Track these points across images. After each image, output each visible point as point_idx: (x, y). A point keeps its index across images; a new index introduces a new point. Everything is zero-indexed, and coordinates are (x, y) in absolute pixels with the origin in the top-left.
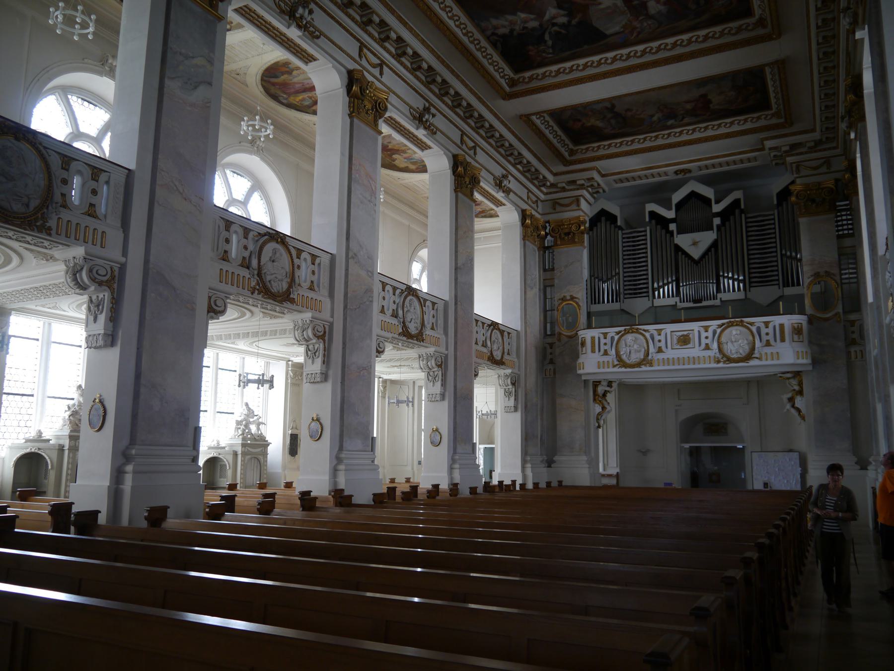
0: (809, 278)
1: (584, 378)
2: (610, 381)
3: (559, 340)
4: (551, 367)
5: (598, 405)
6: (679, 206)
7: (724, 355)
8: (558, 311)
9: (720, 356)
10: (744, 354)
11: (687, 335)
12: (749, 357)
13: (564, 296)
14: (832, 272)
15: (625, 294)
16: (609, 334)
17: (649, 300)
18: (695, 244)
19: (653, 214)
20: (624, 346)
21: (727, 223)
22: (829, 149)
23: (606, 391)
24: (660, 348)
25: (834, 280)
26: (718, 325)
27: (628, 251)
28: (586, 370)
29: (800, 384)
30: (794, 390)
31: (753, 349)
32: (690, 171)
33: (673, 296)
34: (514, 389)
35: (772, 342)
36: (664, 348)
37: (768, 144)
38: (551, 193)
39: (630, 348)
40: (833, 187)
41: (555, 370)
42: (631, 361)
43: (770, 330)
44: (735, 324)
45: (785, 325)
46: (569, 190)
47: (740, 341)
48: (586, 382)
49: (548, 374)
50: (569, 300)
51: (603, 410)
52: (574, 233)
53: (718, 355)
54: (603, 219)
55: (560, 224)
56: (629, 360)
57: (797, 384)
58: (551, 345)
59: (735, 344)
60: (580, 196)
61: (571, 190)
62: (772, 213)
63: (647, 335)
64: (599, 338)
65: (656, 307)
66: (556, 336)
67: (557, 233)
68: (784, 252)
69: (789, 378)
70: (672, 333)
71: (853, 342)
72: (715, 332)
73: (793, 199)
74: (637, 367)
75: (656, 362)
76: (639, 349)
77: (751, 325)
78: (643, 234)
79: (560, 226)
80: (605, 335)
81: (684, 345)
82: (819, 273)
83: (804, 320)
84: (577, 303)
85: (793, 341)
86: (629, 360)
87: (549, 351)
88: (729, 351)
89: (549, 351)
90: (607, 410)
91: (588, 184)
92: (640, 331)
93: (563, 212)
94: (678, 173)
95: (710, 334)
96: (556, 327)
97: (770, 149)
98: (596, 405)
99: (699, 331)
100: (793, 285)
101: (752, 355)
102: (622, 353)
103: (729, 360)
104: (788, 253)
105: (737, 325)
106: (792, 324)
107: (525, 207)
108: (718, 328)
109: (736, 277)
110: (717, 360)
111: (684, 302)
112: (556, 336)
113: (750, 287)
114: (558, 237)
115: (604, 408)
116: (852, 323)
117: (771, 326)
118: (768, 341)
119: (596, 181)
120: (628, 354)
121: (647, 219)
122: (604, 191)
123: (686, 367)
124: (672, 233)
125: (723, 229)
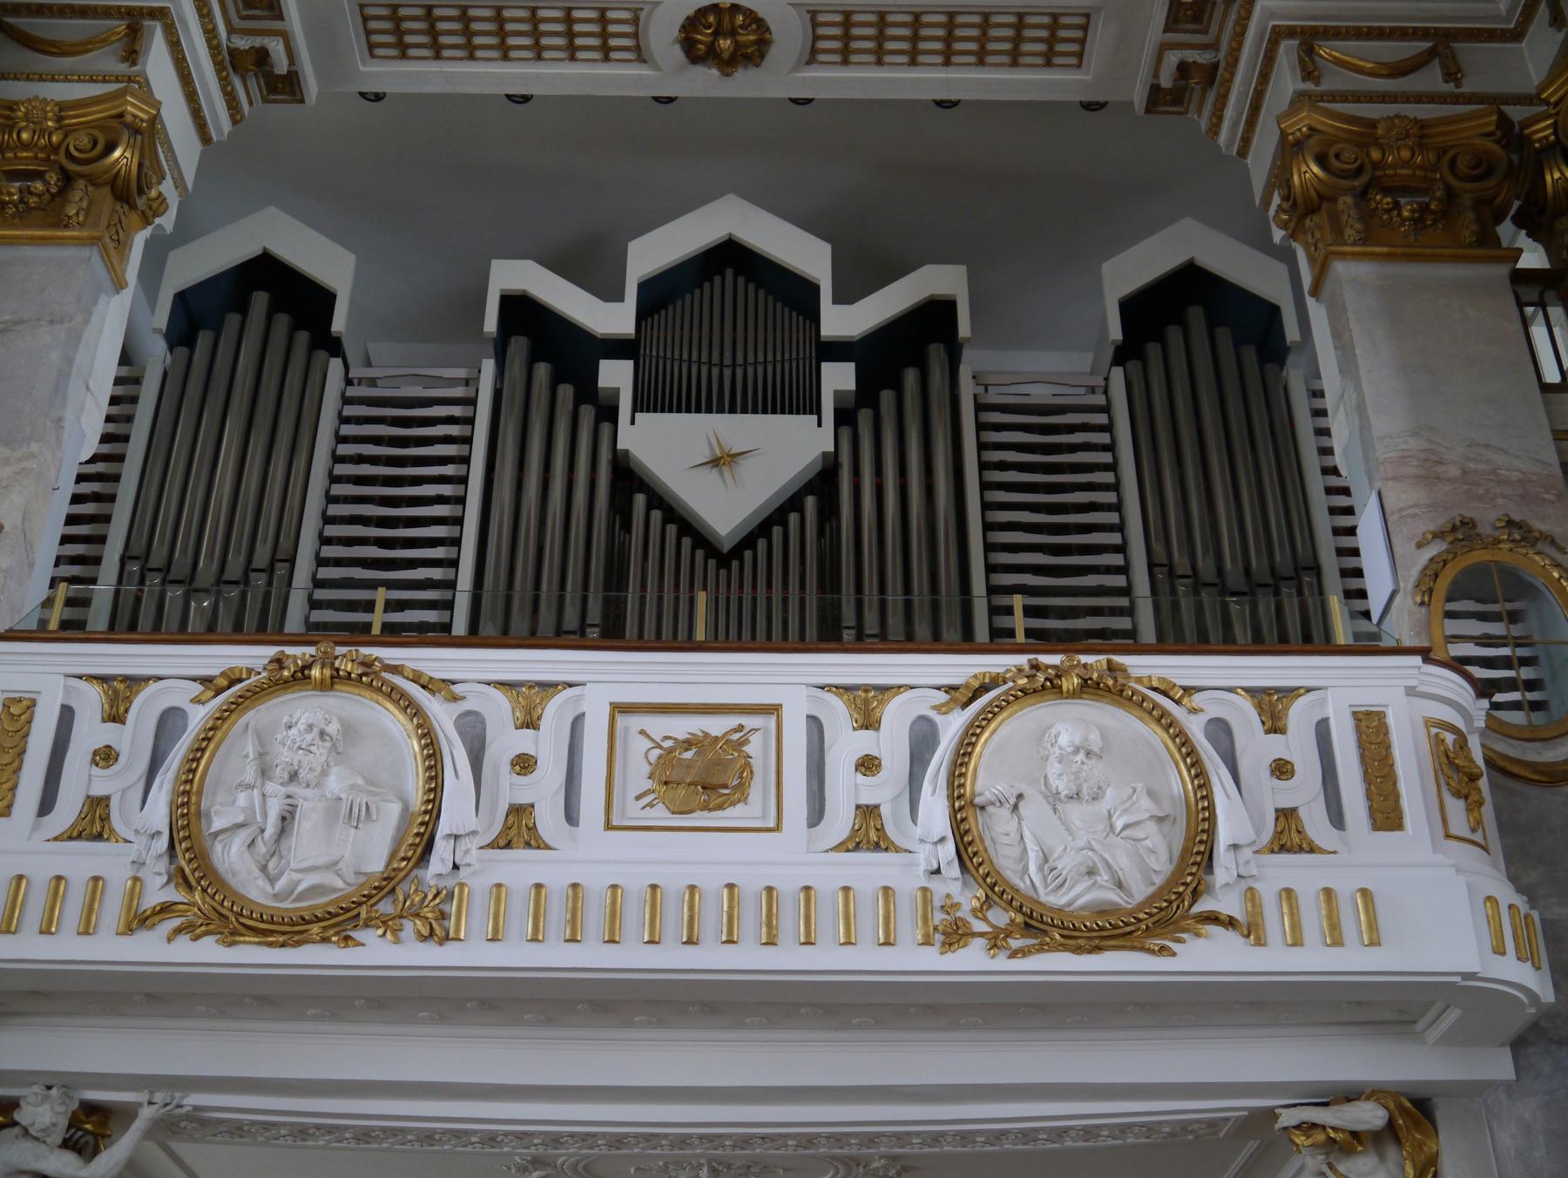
0: (1419, 546)
2: (91, 1109)
7: (996, 890)
9: (968, 898)
10: (1140, 891)
14: (1538, 525)
16: (153, 687)
18: (721, 461)
19: (519, 309)
20: (250, 774)
21: (887, 397)
24: (520, 812)
26: (951, 689)
27: (360, 459)
35: (1315, 822)
36: (548, 819)
39: (292, 789)
40: (1489, 144)
42: (281, 884)
43: (1298, 744)
45: (1391, 720)
47: (1109, 792)
53: (954, 888)
54: (260, 300)
56: (272, 880)
59: (1076, 813)
63: (442, 714)
64: (67, 715)
70: (621, 721)
72: (923, 740)
74: (325, 940)
76: (362, 799)
81: (706, 807)
82: (1468, 524)
85: (1448, 836)
86: (272, 880)
95: (891, 741)
99: (814, 723)
101: (1196, 895)
102: (218, 824)
110: (938, 917)
117: (1299, 715)
118: (1286, 815)
120: (271, 830)
121: (491, 324)
125: (864, 417)
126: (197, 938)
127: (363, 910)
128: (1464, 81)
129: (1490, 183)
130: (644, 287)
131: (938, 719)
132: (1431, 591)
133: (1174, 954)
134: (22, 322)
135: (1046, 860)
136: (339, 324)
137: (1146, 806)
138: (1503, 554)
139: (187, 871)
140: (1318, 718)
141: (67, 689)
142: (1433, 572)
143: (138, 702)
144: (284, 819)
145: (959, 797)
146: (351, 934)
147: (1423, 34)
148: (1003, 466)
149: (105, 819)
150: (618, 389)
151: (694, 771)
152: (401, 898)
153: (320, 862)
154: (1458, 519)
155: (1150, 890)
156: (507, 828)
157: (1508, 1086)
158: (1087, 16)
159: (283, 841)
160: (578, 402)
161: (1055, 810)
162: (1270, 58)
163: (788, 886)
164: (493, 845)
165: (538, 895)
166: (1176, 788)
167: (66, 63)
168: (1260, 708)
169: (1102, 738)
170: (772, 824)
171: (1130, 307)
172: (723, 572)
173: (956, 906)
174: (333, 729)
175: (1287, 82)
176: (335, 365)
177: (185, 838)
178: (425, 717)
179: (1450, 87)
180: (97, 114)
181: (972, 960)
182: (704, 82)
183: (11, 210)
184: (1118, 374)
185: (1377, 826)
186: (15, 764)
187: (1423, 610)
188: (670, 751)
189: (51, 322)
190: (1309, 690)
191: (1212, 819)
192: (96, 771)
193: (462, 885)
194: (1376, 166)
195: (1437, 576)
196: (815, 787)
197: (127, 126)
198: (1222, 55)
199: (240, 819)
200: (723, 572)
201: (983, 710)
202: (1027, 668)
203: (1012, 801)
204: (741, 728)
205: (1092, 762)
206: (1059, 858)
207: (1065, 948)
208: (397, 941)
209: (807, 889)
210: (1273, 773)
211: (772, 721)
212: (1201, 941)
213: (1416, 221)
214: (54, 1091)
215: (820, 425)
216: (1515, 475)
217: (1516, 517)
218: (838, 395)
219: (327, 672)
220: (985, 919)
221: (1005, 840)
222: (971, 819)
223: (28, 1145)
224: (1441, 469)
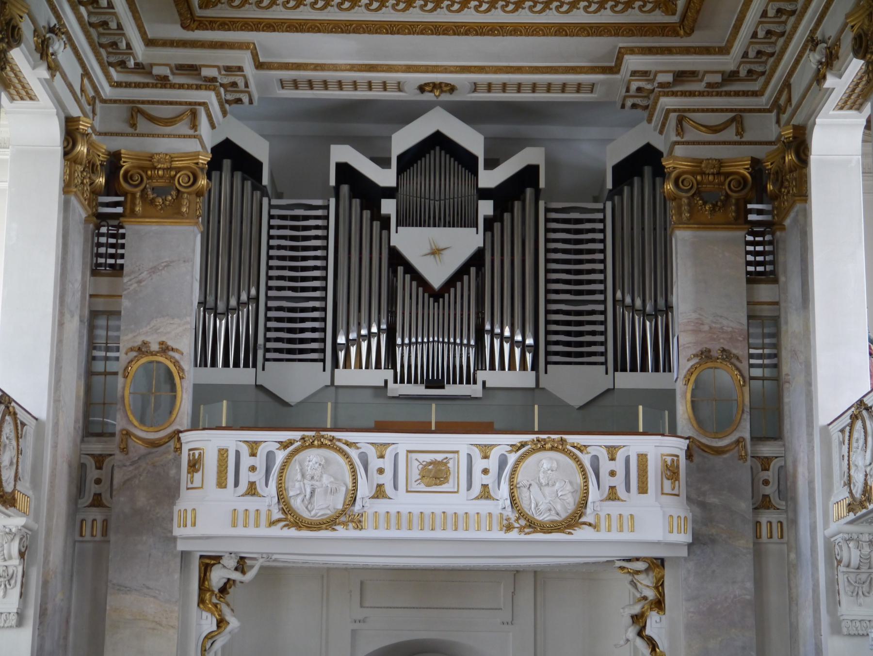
0: (688, 360)
1: (181, 546)
3: (124, 450)
4: (96, 514)
5: (209, 615)
6: (407, 161)
7: (522, 514)
8: (126, 377)
9: (512, 515)
10: (564, 515)
11: (443, 463)
12: (573, 521)
13: (145, 343)
14: (734, 351)
15: (267, 350)
16: (263, 445)
17: (324, 370)
18: (436, 252)
19: (345, 172)
20: (299, 477)
21: (507, 216)
22: (745, 94)
23: (229, 580)
25: (738, 369)
26: (512, 446)
27: (280, 247)
28: (201, 530)
29: (659, 586)
30: (645, 598)
31: (583, 503)
32: (452, 89)
33: (378, 366)
34: (20, 569)
35: (621, 491)
36: (389, 489)
37: (633, 62)
38: (128, 85)
39: (314, 482)
41: (105, 522)
42: (313, 513)
43: (619, 465)
44: (548, 446)
45: (649, 457)
46: (173, 86)
47: (557, 484)
48: (185, 556)
49: (87, 531)
50: (152, 354)
51: (218, 626)
52: (178, 191)
54: (227, 163)
55: (148, 164)
56: (310, 511)
57: (650, 585)
58: (100, 460)
59: (547, 490)
60: (200, 104)
61: (181, 86)
62: (600, 206)
63: (354, 454)
64: (238, 454)
65: (338, 387)
66: (118, 438)
67: (136, 186)
68: (619, 295)
69: (638, 572)
70: (410, 455)
71: (764, 504)
73: (669, 186)
74: (326, 529)
75: (371, 518)
76: (334, 486)
77: (581, 451)
78: (319, 213)
79: (144, 169)
81: (436, 484)
83: (681, 449)
84: (176, 363)
85: (663, 494)
86: (310, 511)
87: (93, 473)
88: (533, 506)
89: (93, 473)
90: (229, 628)
91: (225, 81)
92: (338, 443)
93: (153, 136)
94: (427, 88)
95: (492, 463)
96: (118, 416)
97: (634, 73)
98: (205, 614)
99: (469, 457)
100: (634, 369)
101: (580, 517)
102: (291, 493)
103: (533, 525)
104: (628, 300)
105: (553, 448)
106: (662, 455)
107: (75, 112)
108: (510, 452)
109: (519, 338)
110: (505, 522)
111: (402, 382)
112: (118, 438)
113: (547, 363)
114: (138, 195)
115: (221, 623)
116: (765, 463)
117: (620, 455)
118: (612, 488)
119: (244, 76)
120: (308, 497)
121: (332, 182)
122: (251, 102)
123: (439, 534)
124: (385, 222)
125: (497, 226)
126: (289, 528)
127: (337, 520)
128: (745, 135)
129: (746, 191)
130: (400, 158)
132: (689, 380)
134: (173, 262)
135: (537, 506)
136: (265, 181)
137: (569, 487)
139: (284, 508)
141: (237, 445)
143: (260, 448)
144: (312, 493)
145: (512, 485)
147: (732, 110)
148: (556, 251)
149: (255, 489)
151: (432, 473)
152: (348, 516)
153: (324, 506)
154: (704, 349)
155: (567, 514)
156: (377, 491)
157: (685, 558)
160: (372, 219)
161: (541, 489)
163: (461, 513)
164: (373, 497)
165: (388, 516)
167: (168, 130)
169: (557, 464)
170: (456, 490)
171: (616, 169)
174: (322, 463)
177: (283, 498)
178: (351, 459)
179: (737, 138)
185: (640, 493)
186: (225, 471)
187: (686, 387)
188: (425, 466)
189: (184, 261)
192: (250, 473)
195: (692, 374)
196: (469, 477)
198: (650, 102)
199: (298, 492)
200: (436, 304)
201: (523, 454)
202: (535, 439)
204: (447, 458)
206: (541, 505)
207: (541, 532)
209: (466, 513)
210: (609, 475)
211: (456, 455)
212: (581, 530)
213: (711, 211)
214: (233, 555)
215: (477, 233)
216: (730, 329)
217: (726, 348)
219: (319, 443)
220: (518, 523)
221: (525, 499)
222: (515, 492)
223: (225, 570)
224: (702, 327)
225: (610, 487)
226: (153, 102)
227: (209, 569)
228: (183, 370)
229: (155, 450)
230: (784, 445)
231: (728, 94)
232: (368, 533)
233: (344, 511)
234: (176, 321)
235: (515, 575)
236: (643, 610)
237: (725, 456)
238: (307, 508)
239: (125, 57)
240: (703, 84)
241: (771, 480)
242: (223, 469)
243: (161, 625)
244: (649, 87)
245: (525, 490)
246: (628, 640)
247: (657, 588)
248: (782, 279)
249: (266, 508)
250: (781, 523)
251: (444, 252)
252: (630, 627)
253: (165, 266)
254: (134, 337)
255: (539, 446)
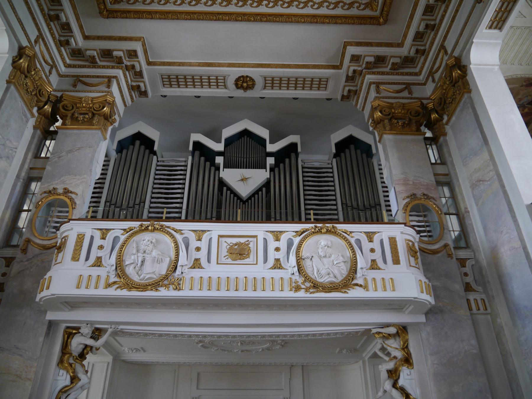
0: (403, 199)
2: (97, 329)
5: (65, 372)
7: (307, 278)
9: (300, 280)
10: (340, 278)
13: (54, 189)
14: (431, 195)
16: (112, 231)
18: (244, 180)
19: (198, 145)
20: (134, 251)
21: (282, 165)
22: (411, 74)
23: (86, 346)
26: (296, 232)
27: (160, 179)
29: (405, 348)
30: (395, 357)
31: (353, 270)
36: (204, 262)
37: (352, 50)
38: (75, 66)
39: (144, 255)
40: (419, 109)
42: (141, 277)
43: (376, 245)
45: (397, 239)
46: (99, 67)
47: (333, 256)
48: (52, 325)
51: (72, 382)
53: (297, 277)
54: (138, 143)
56: (139, 276)
59: (325, 260)
61: (104, 67)
64: (92, 238)
70: (221, 239)
72: (290, 244)
74: (152, 290)
80: (104, 233)
81: (240, 259)
84: (71, 199)
85: (410, 266)
86: (139, 276)
90: (80, 384)
95: (283, 244)
98: (62, 372)
99: (265, 239)
101: (353, 279)
102: (127, 263)
103: (316, 286)
110: (294, 284)
115: (74, 379)
116: (462, 262)
117: (376, 238)
118: (373, 261)
120: (139, 264)
121: (191, 148)
125: (276, 170)
126: (122, 289)
127: (161, 283)
129: (419, 117)
130: (226, 140)
131: (293, 239)
133: (348, 293)
134: (83, 147)
135: (318, 271)
136: (156, 148)
137: (341, 259)
138: (422, 202)
139: (120, 274)
140: (381, 239)
141: (92, 231)
142: (406, 205)
144: (142, 262)
145: (298, 257)
146: (158, 288)
147: (404, 84)
148: (308, 181)
149: (101, 262)
150: (220, 163)
151: (237, 251)
152: (169, 280)
153: (151, 272)
155: (342, 278)
156: (194, 264)
158: (328, 79)
159: (142, 267)
160: (211, 166)
161: (320, 260)
162: (369, 89)
165: (201, 279)
166: (348, 255)
168: (367, 236)
170: (255, 263)
171: (337, 145)
172: (244, 205)
173: (298, 282)
174: (154, 241)
175: (373, 94)
176: (155, 157)
177: (119, 266)
178: (175, 238)
179: (410, 96)
180: (100, 100)
181: (301, 294)
182: (240, 93)
183: (80, 122)
184: (334, 160)
187: (404, 214)
188: (232, 246)
189: (90, 147)
190: (378, 232)
191: (356, 262)
192: (99, 251)
193: (183, 277)
194: (393, 113)
195: (407, 206)
196: (265, 254)
197: (107, 102)
199: (132, 262)
200: (244, 205)
201: (304, 237)
202: (314, 227)
203: (311, 258)
204: (248, 241)
205: (329, 249)
206: (322, 271)
208: (168, 290)
209: (263, 278)
210: (370, 251)
211: (255, 239)
212: (354, 290)
213: (402, 126)
215: (266, 171)
216: (425, 184)
217: (425, 193)
218: (270, 165)
219: (153, 228)
220: (304, 285)
221: (309, 267)
222: (301, 262)
223: (82, 337)
224: (408, 182)
225: (371, 260)
226: (88, 76)
227: (71, 336)
228: (75, 203)
229: (45, 252)
230: (473, 251)
231: (402, 74)
232: (185, 293)
233: (166, 276)
234: (78, 177)
235: (290, 368)
236: (396, 366)
237: (439, 255)
238: (138, 273)
239: (68, 38)
240: (390, 66)
241: (468, 273)
242: (78, 248)
243: (20, 378)
244: (360, 69)
245: (309, 260)
246: (385, 391)
247: (403, 349)
248: (448, 160)
249: (106, 274)
250: (484, 300)
251: (247, 179)
252: (387, 380)
253: (78, 149)
254: (49, 186)
255: (317, 229)
